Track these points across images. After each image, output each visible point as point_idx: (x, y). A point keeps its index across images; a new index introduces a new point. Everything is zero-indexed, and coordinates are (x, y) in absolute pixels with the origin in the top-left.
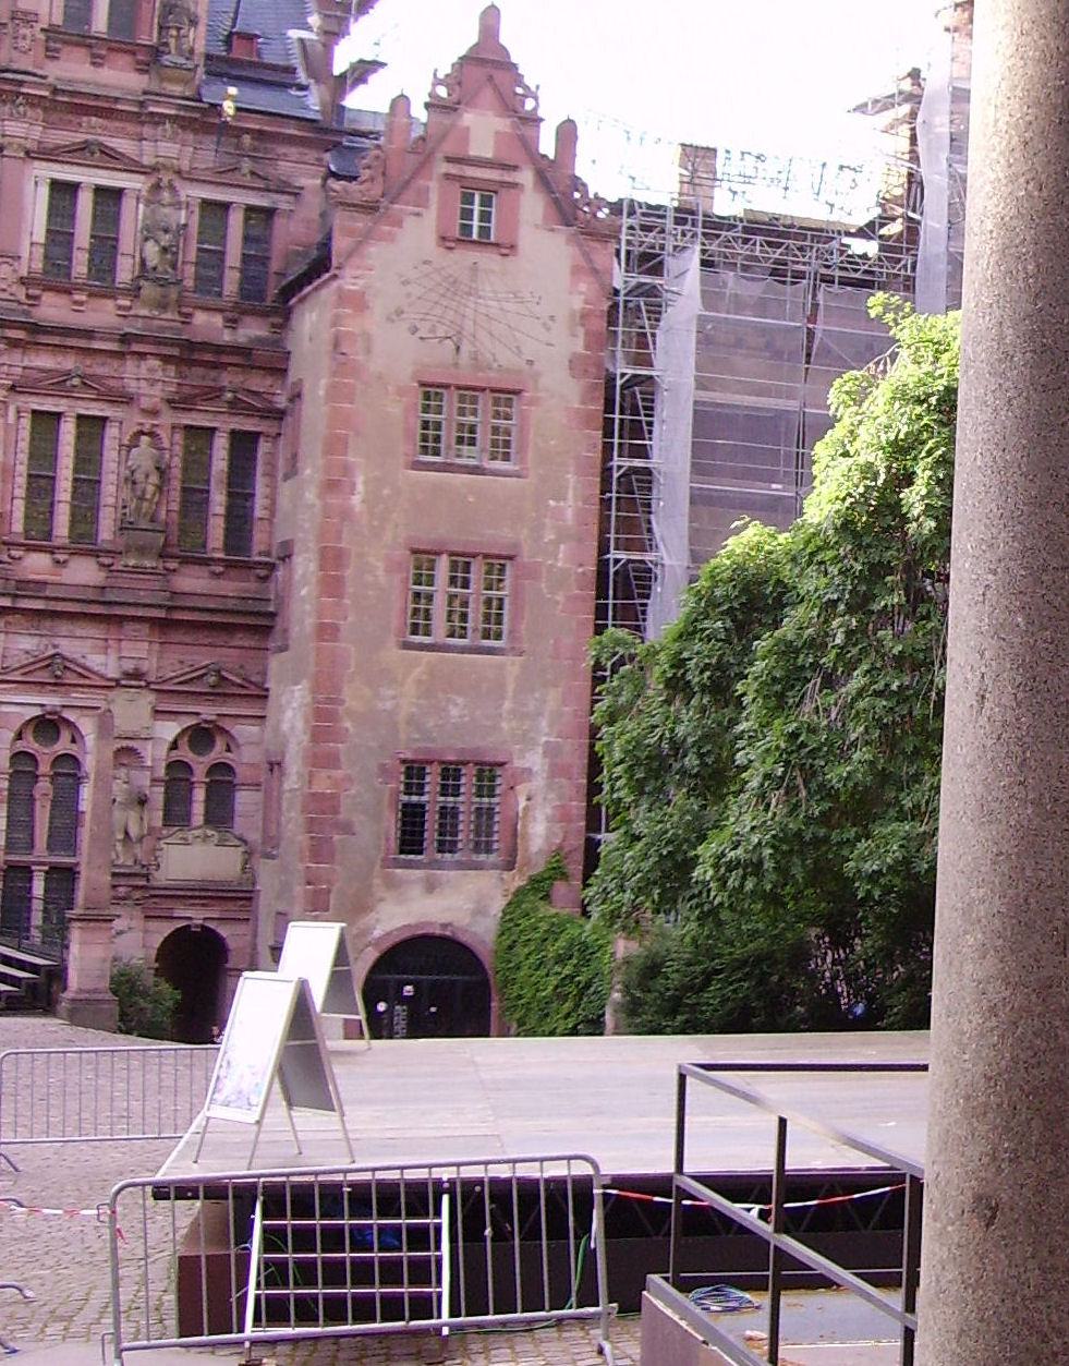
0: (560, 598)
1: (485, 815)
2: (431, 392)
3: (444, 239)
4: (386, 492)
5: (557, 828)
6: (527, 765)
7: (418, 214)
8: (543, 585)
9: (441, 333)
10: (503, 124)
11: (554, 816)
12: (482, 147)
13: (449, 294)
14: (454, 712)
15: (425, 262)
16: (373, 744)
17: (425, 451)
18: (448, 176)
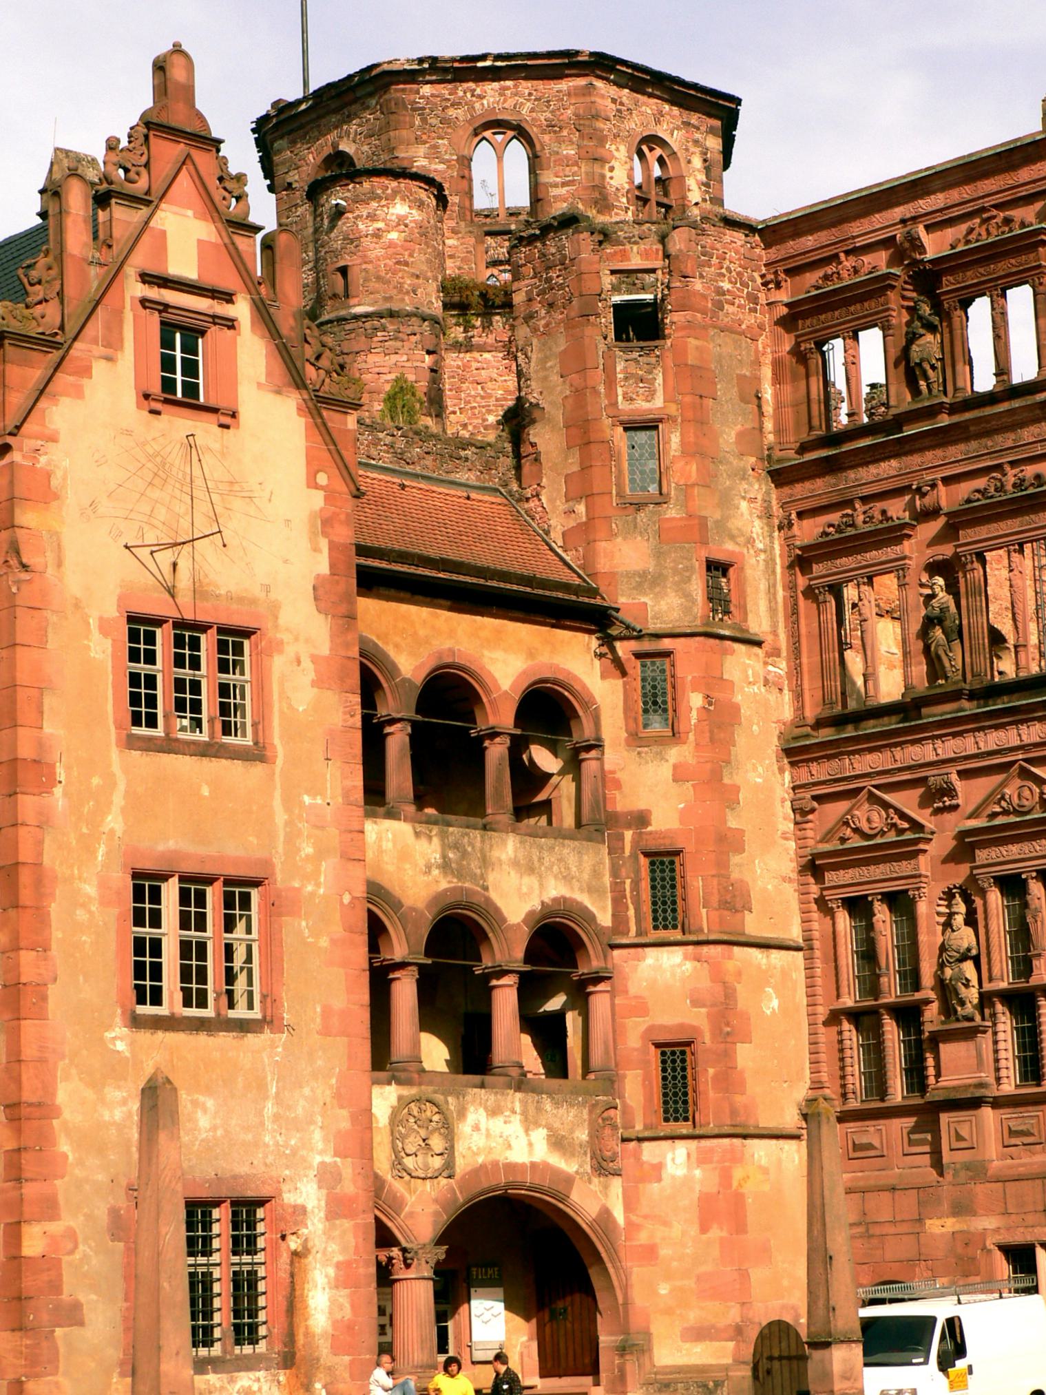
0: (324, 942)
1: (244, 1285)
2: (140, 630)
3: (147, 396)
4: (96, 781)
5: (343, 1296)
6: (300, 1201)
7: (109, 359)
8: (304, 923)
9: (150, 538)
10: (206, 231)
11: (336, 1279)
12: (183, 265)
13: (157, 481)
14: (204, 1122)
15: (129, 433)
16: (100, 1177)
17: (136, 721)
18: (144, 302)
